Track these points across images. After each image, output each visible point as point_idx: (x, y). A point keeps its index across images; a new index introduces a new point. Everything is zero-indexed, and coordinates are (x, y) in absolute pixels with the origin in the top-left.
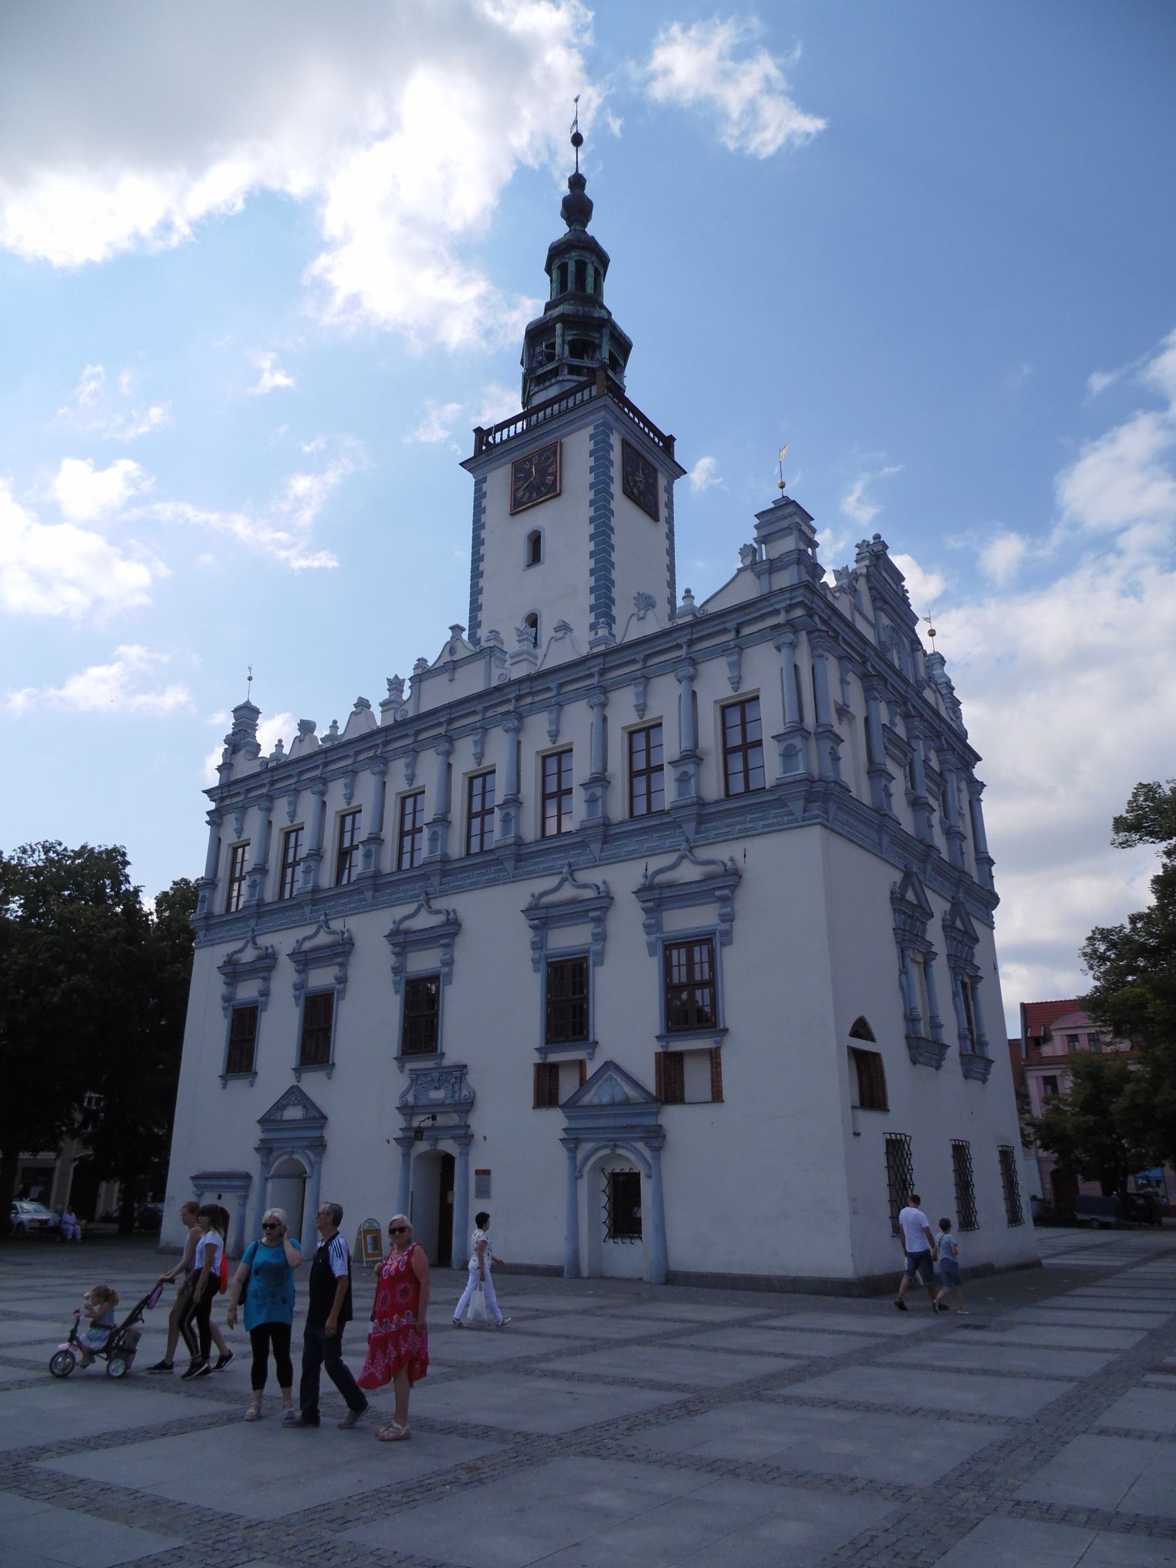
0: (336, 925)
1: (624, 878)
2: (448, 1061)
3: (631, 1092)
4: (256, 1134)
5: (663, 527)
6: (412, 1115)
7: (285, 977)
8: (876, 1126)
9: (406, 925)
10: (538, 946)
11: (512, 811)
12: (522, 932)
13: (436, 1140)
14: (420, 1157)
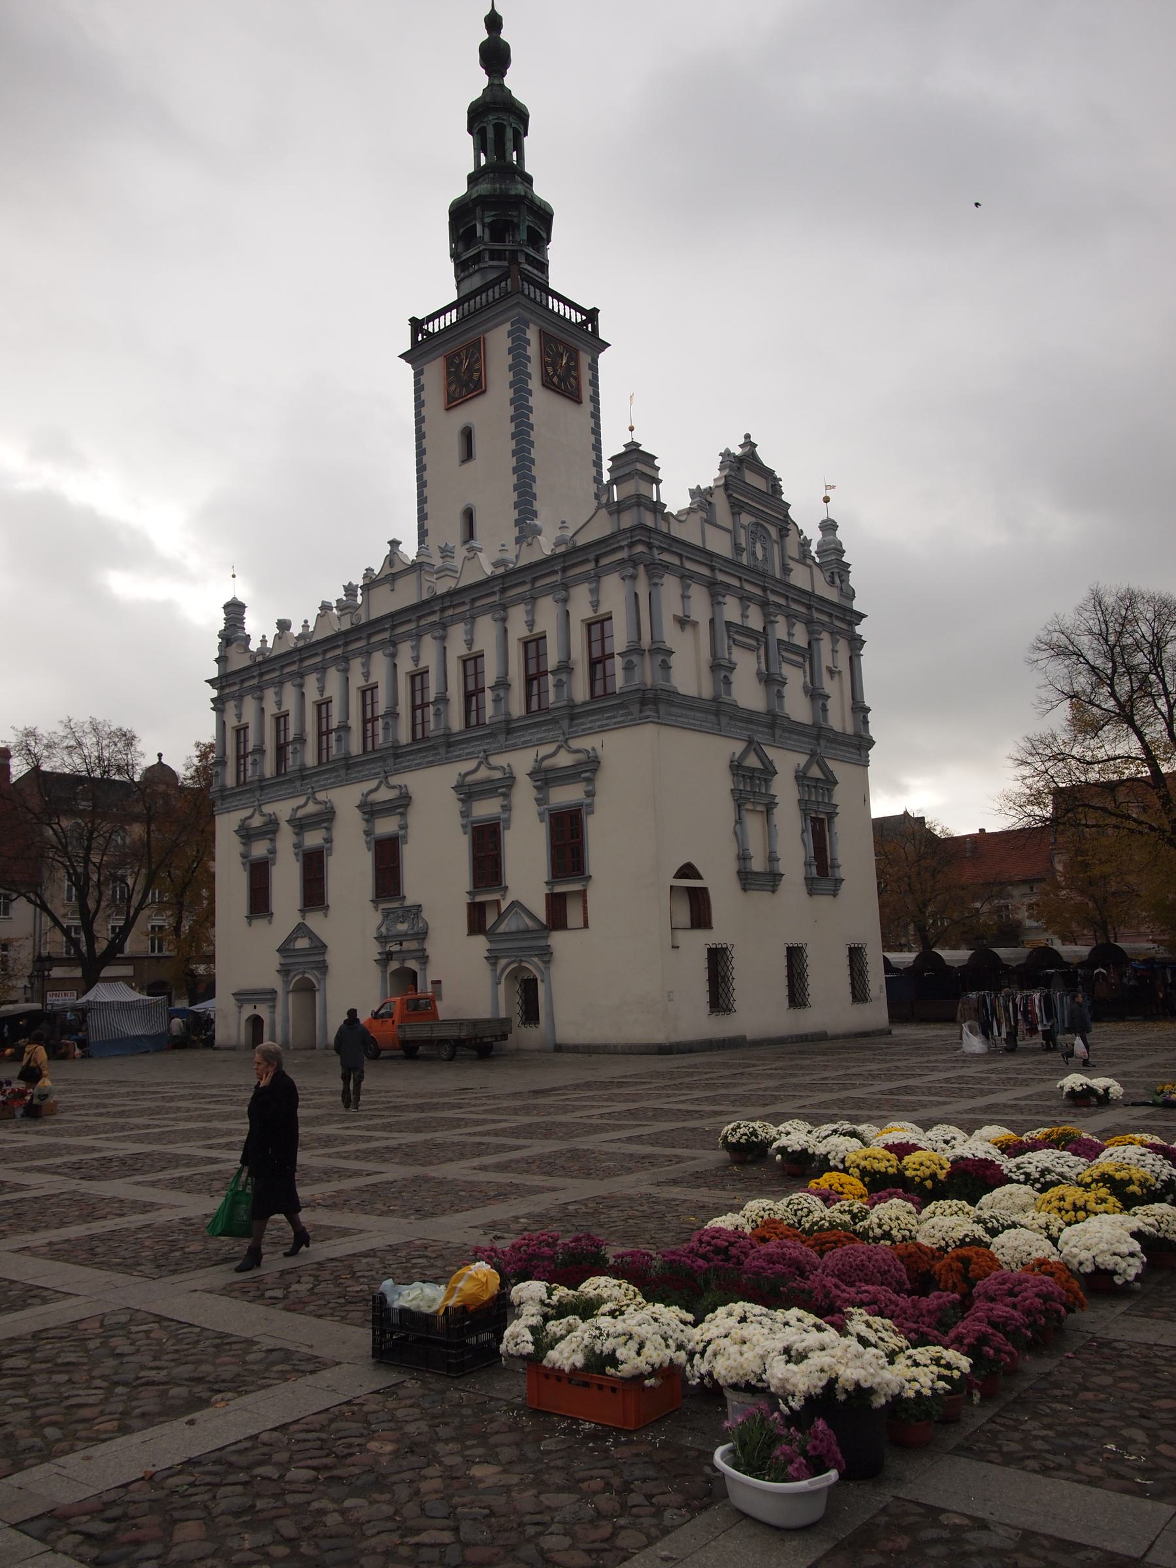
0: (321, 796)
1: (521, 762)
2: (408, 902)
3: (530, 923)
4: (276, 960)
5: (588, 406)
6: (386, 943)
7: (286, 839)
8: (697, 943)
9: (371, 798)
10: (465, 814)
11: (441, 707)
12: (452, 804)
13: (404, 960)
14: (394, 973)
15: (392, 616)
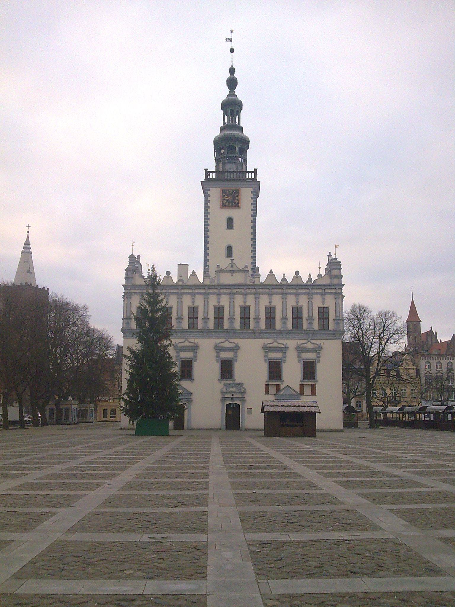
0: (192, 340)
1: (292, 344)
2: (236, 382)
3: (294, 393)
9: (220, 345)
15: (235, 285)
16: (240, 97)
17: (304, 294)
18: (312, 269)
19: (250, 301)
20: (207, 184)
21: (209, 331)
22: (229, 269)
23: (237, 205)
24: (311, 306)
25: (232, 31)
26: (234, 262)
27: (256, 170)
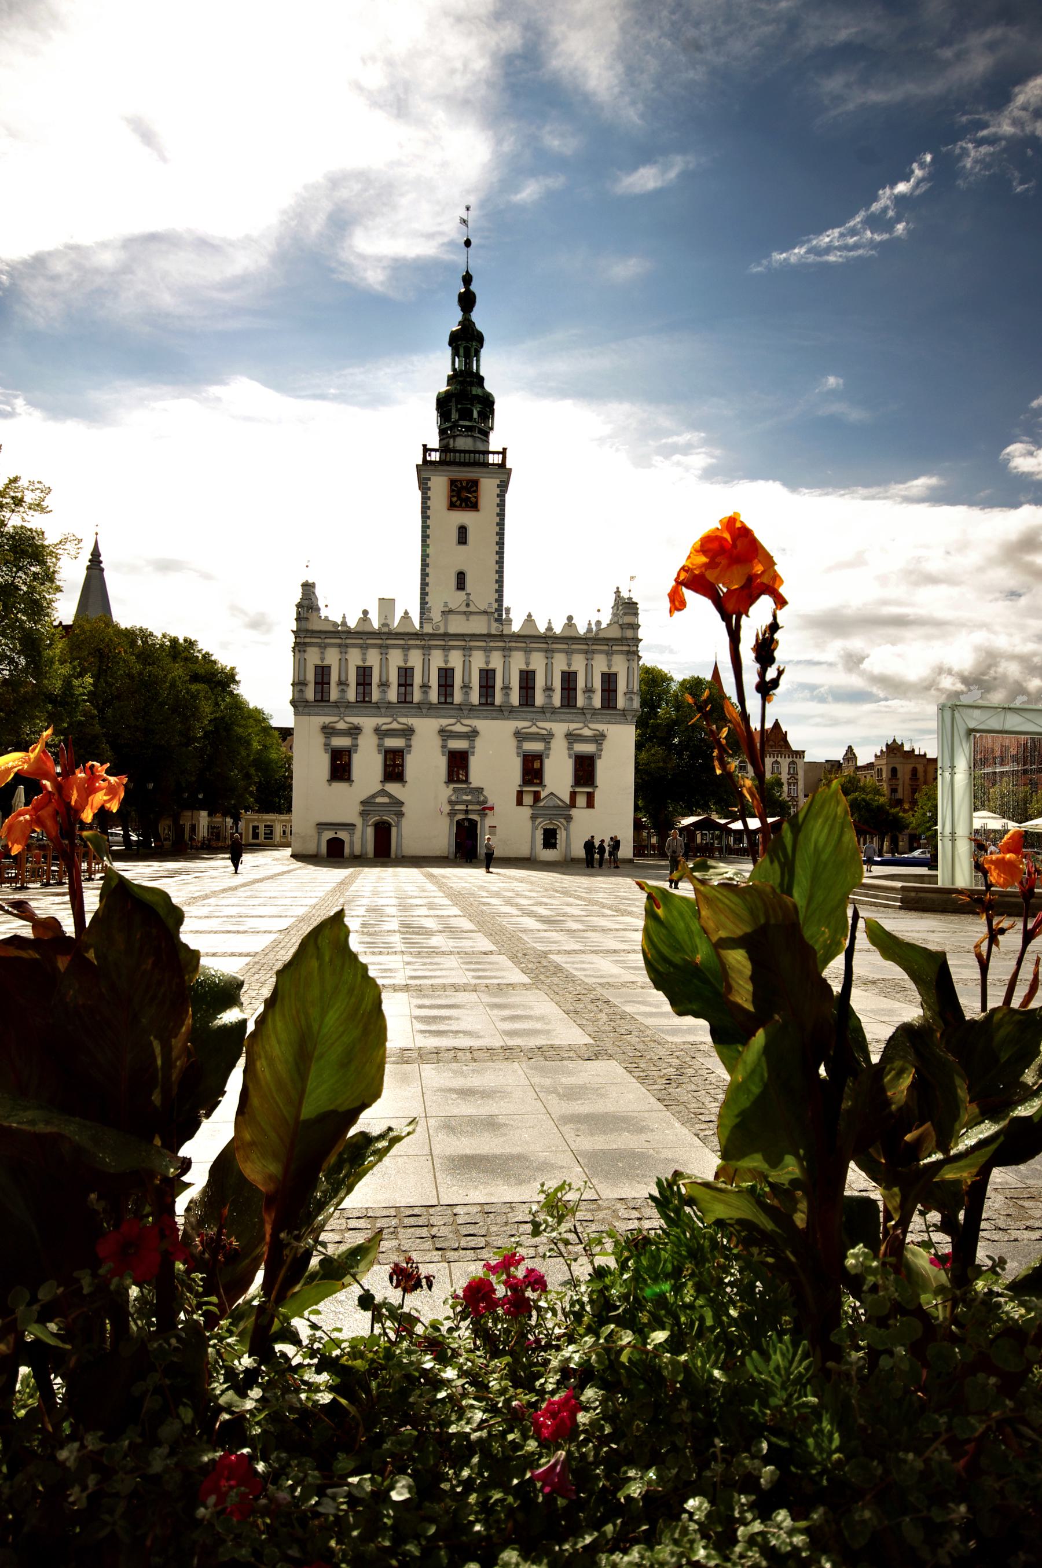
1: (559, 728)
3: (560, 803)
4: (358, 808)
10: (519, 747)
15: (474, 635)
16: (480, 326)
17: (579, 651)
18: (593, 612)
19: (496, 662)
20: (425, 468)
21: (430, 706)
22: (464, 609)
23: (473, 505)
24: (590, 672)
25: (468, 209)
26: (471, 597)
27: (505, 449)
